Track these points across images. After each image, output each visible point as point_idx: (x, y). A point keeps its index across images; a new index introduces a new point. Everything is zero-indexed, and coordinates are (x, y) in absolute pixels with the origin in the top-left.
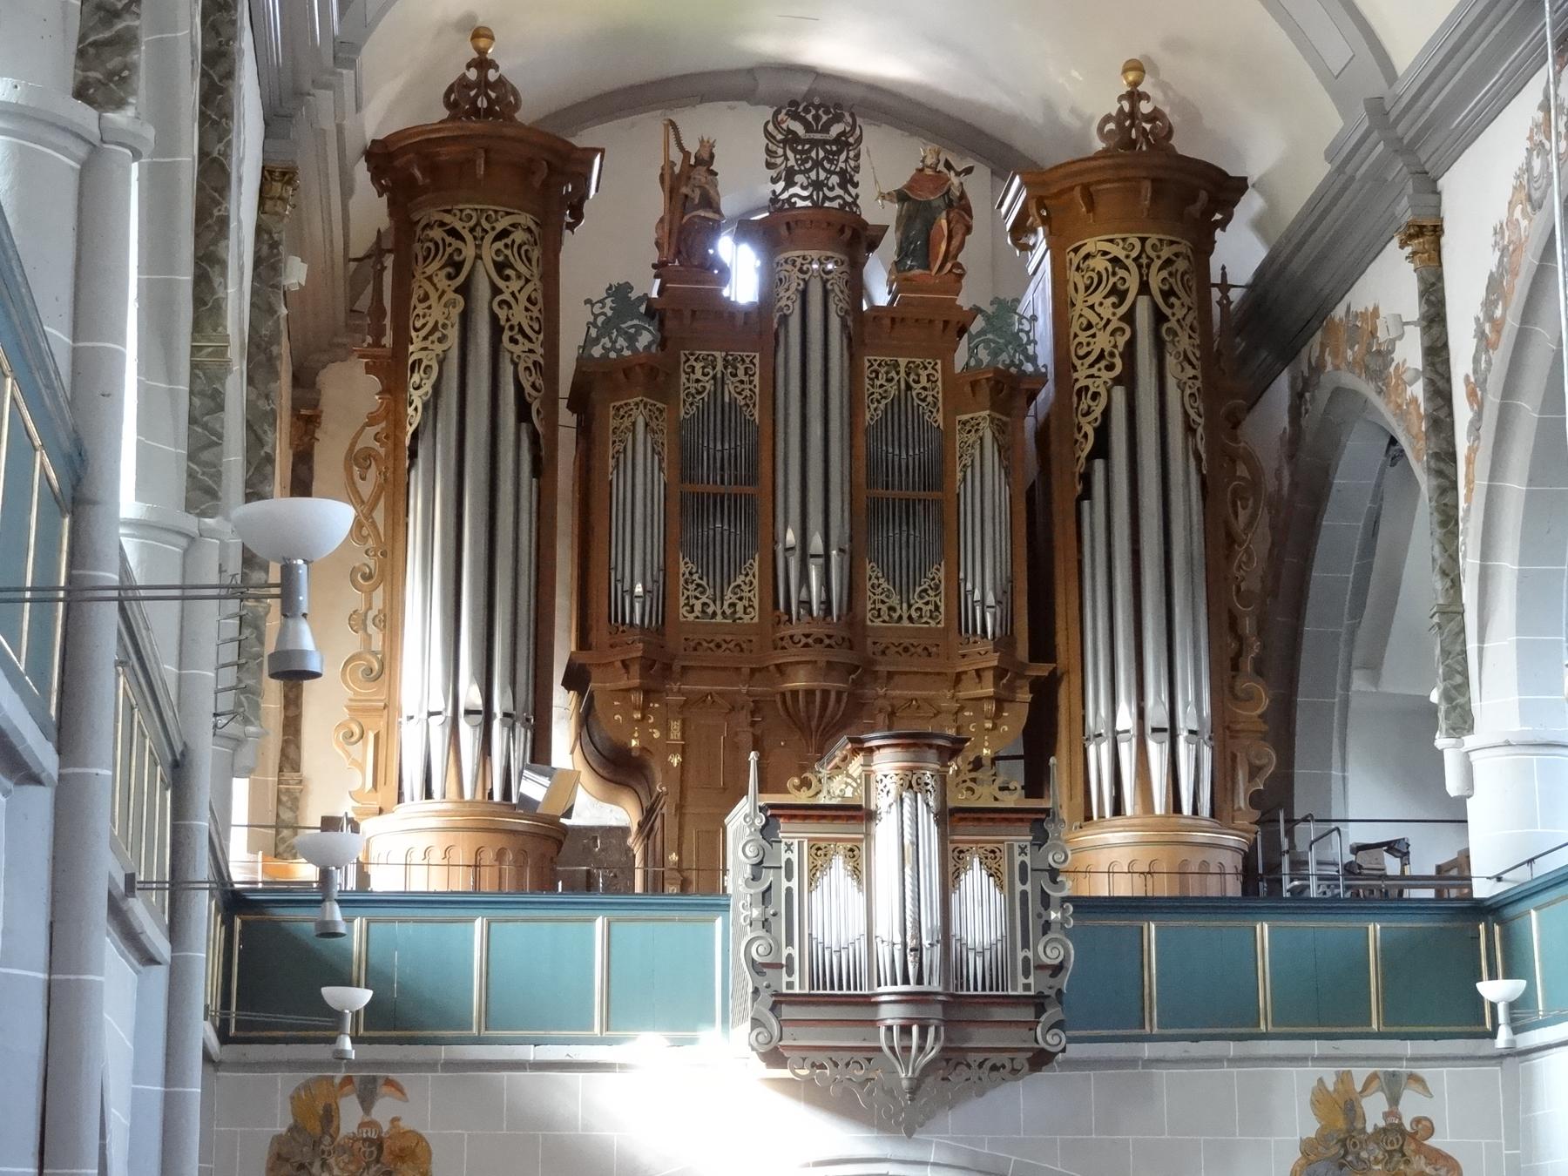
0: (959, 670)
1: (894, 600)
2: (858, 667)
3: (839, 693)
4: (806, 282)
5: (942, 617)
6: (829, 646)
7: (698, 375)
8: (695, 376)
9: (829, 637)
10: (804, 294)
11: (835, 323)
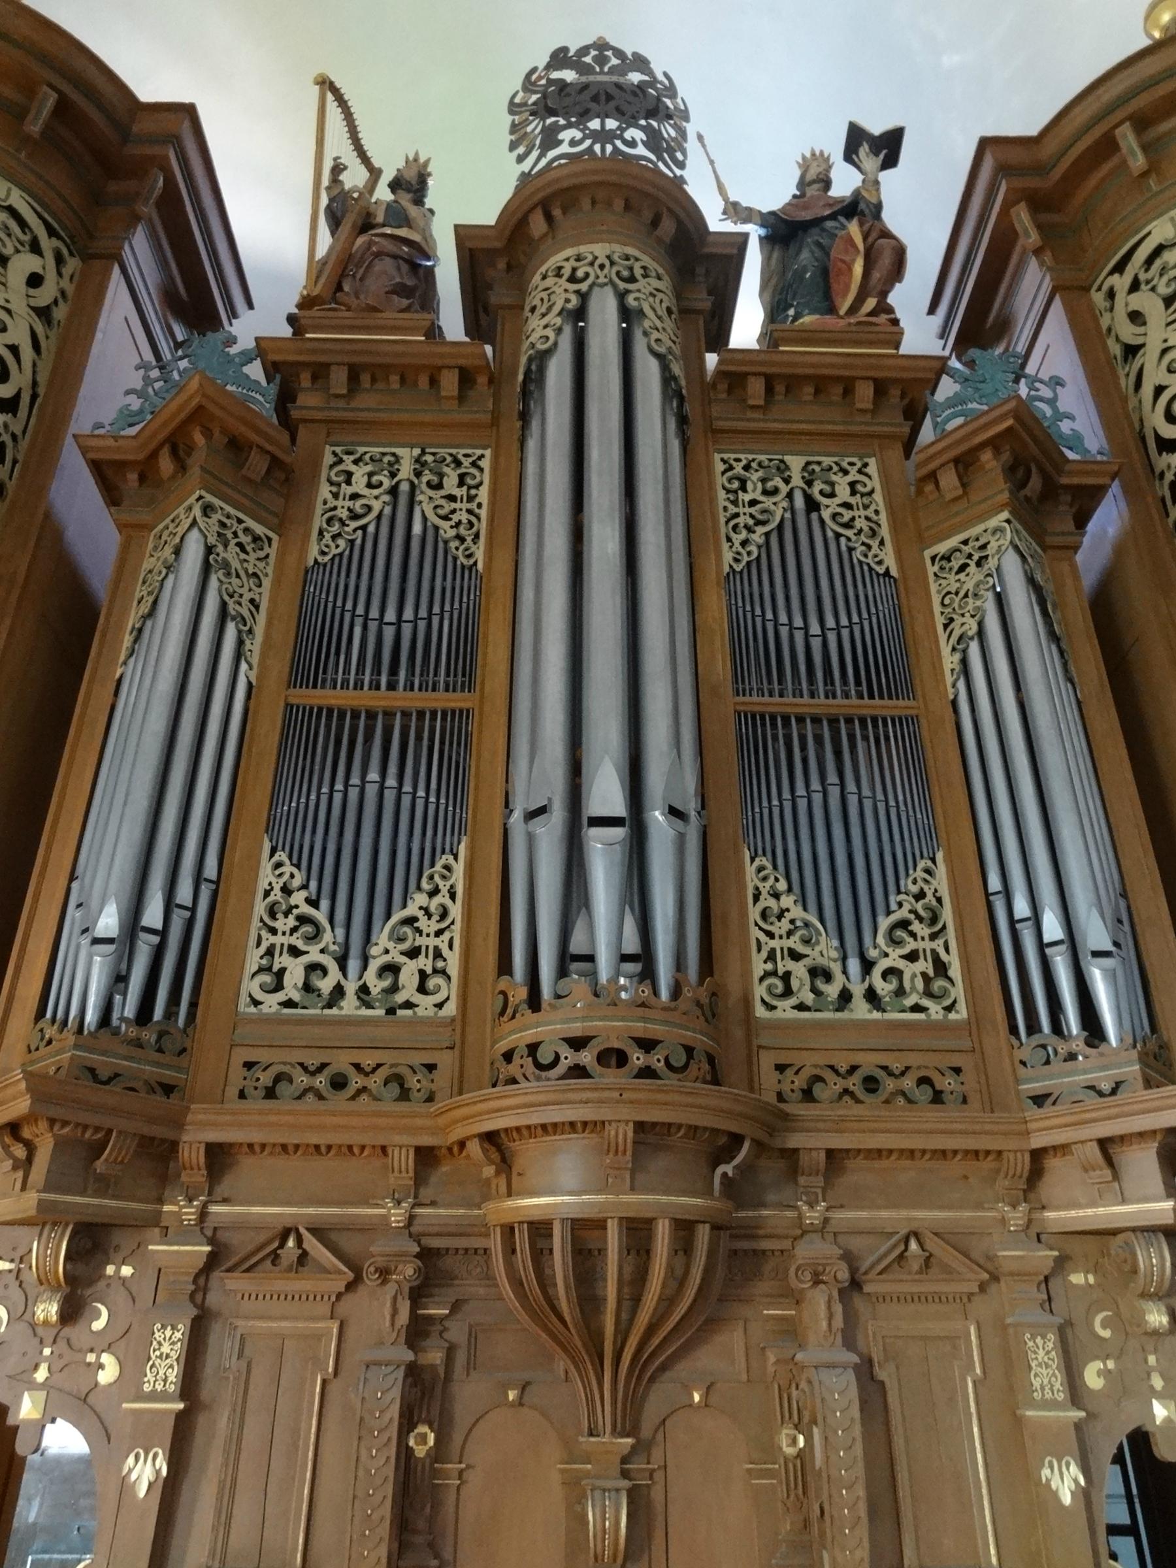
0: (1037, 1142)
1: (825, 951)
2: (737, 1140)
3: (684, 1228)
4: (584, 297)
5: (958, 992)
6: (647, 1073)
7: (359, 483)
8: (351, 486)
9: (647, 1045)
10: (579, 314)
11: (648, 372)
